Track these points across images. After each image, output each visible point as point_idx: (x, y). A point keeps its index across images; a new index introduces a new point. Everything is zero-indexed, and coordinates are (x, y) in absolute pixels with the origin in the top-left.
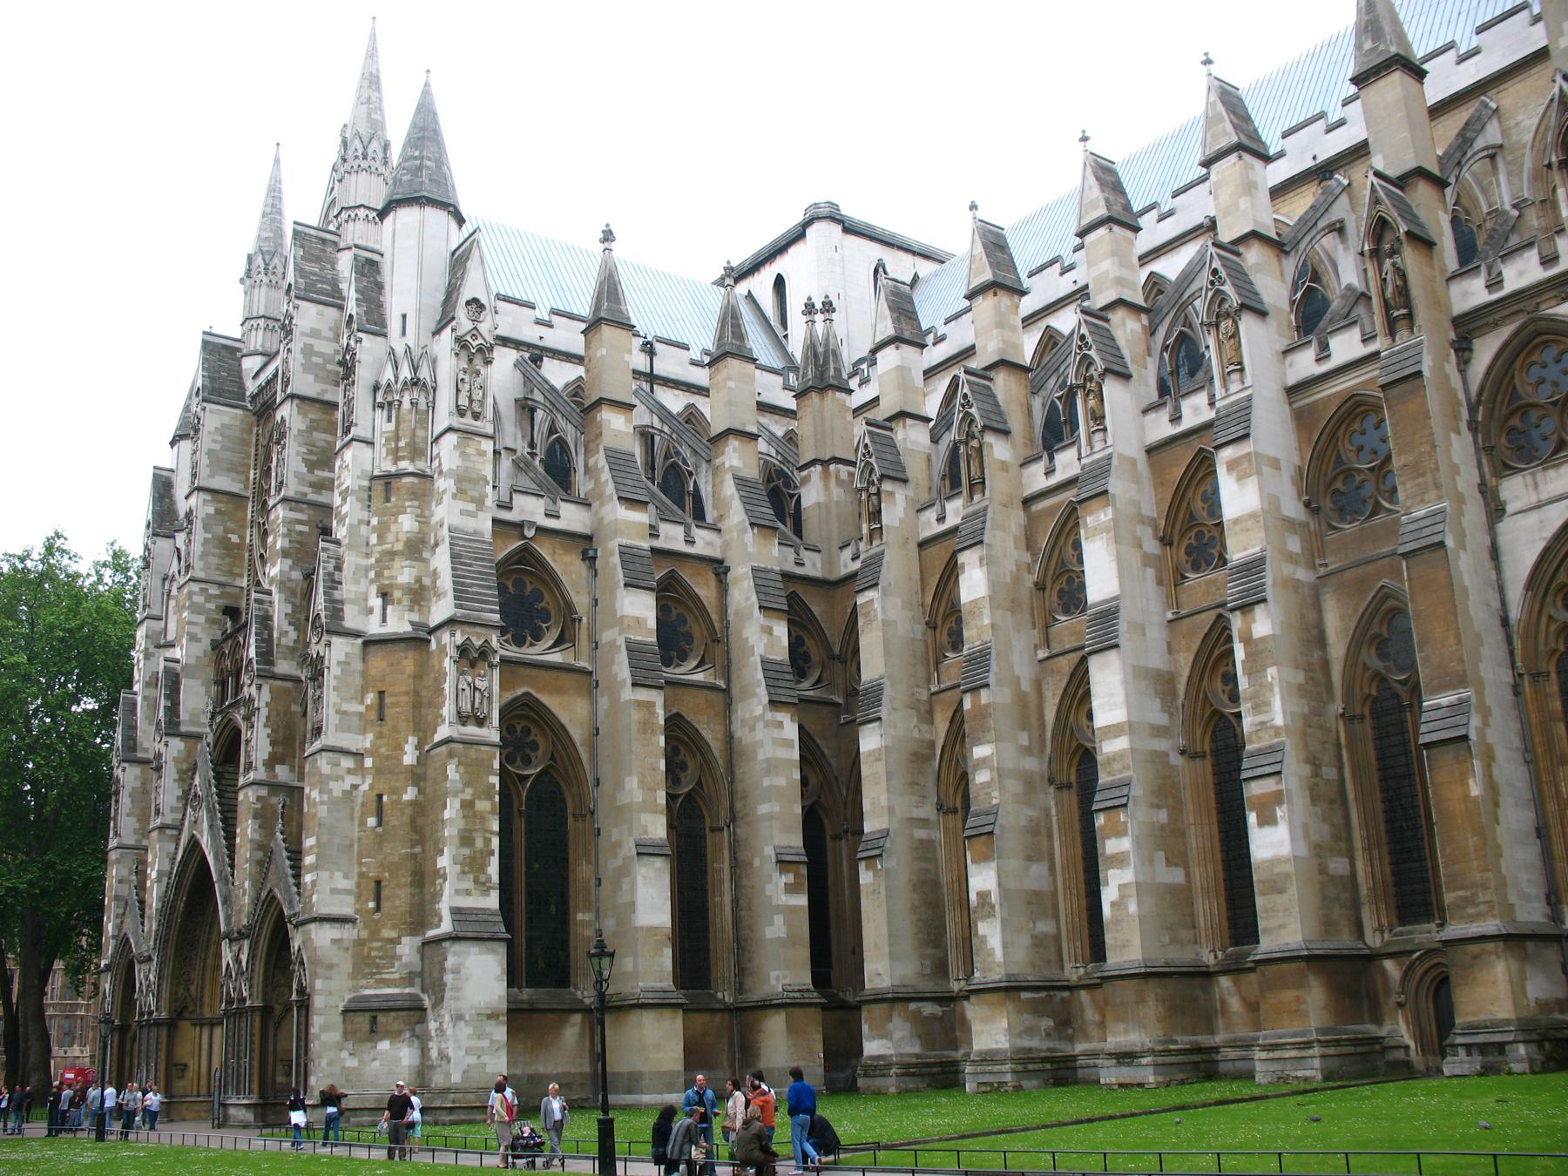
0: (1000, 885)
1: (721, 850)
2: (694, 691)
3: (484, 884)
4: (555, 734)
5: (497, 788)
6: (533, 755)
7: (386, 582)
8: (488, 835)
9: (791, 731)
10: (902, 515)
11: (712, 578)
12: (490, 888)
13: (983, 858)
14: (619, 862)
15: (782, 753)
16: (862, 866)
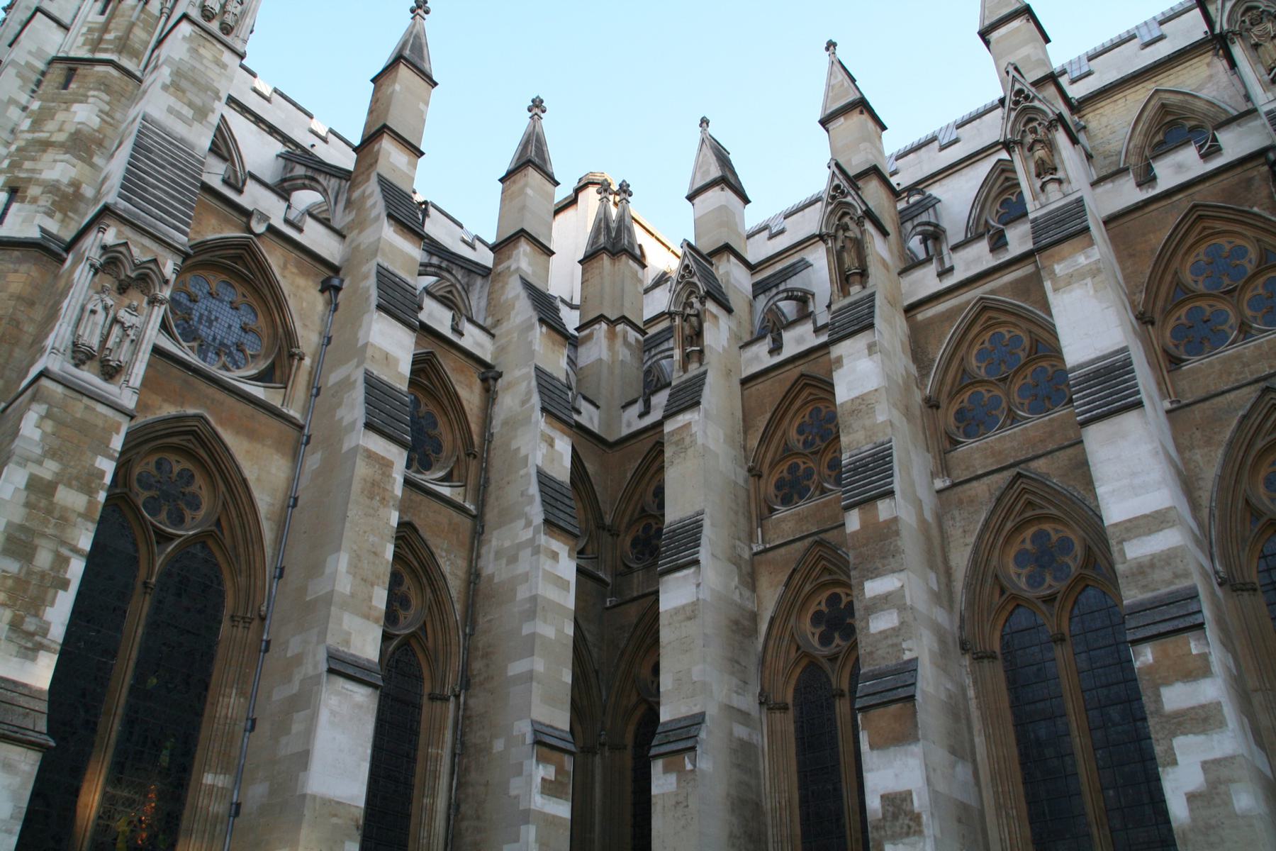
0: (929, 781)
1: (442, 729)
2: (437, 505)
3: (30, 635)
4: (230, 491)
5: (108, 479)
6: (188, 514)
7: (23, 175)
8: (64, 551)
9: (567, 568)
10: (725, 344)
11: (478, 385)
12: (40, 647)
13: (904, 735)
14: (294, 688)
15: (550, 593)
16: (657, 767)
